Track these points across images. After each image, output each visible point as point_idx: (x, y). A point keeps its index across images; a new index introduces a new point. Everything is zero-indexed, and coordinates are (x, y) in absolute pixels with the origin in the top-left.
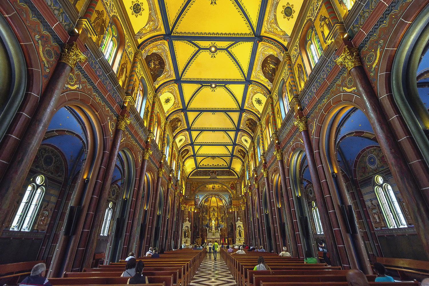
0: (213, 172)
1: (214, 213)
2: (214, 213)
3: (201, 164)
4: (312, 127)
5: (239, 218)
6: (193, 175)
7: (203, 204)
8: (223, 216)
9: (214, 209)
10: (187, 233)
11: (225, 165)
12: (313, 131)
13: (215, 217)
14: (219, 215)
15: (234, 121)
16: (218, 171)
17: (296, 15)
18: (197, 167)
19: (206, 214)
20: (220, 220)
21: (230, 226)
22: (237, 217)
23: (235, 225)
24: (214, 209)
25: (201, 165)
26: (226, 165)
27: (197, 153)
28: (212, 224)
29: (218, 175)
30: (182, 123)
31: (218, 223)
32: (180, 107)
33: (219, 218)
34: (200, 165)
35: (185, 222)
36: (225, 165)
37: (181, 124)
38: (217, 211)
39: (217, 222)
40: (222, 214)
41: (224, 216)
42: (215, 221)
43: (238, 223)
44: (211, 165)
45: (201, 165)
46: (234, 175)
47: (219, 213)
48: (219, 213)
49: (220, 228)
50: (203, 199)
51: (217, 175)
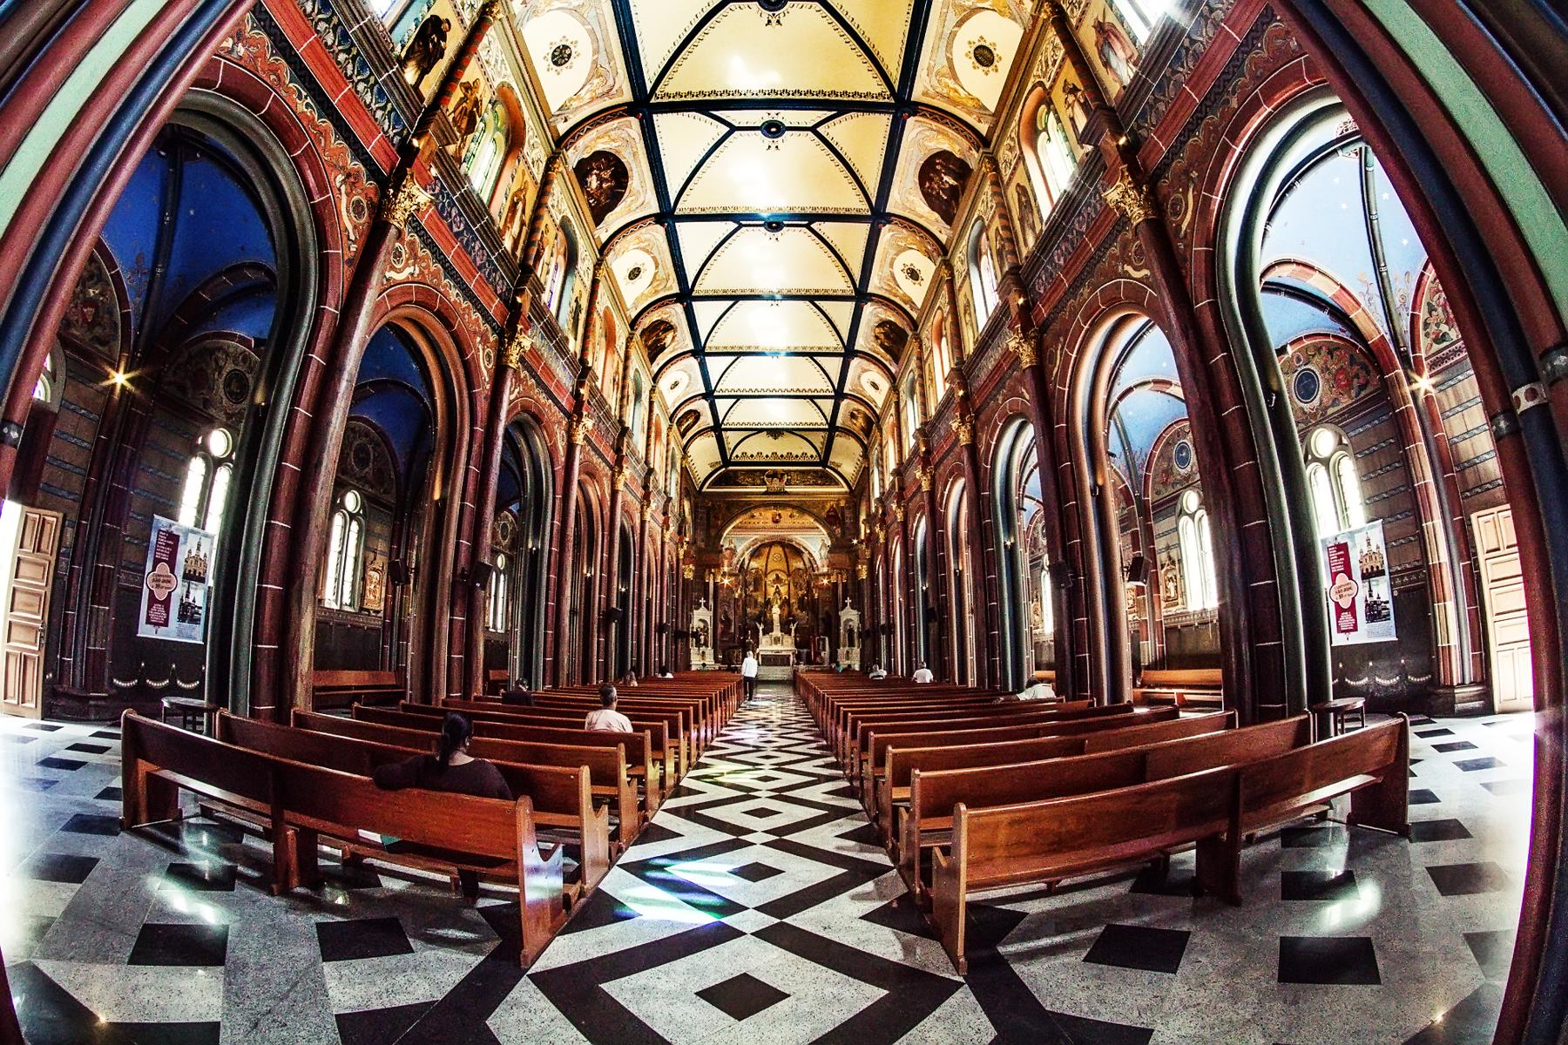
0: (774, 475)
3: (738, 452)
5: (848, 601)
6: (713, 485)
7: (747, 562)
8: (803, 596)
9: (777, 575)
10: (702, 637)
11: (812, 456)
14: (792, 592)
15: (830, 376)
16: (788, 472)
18: (726, 461)
19: (756, 590)
20: (796, 606)
22: (845, 598)
23: (838, 618)
24: (777, 575)
25: (737, 456)
26: (815, 454)
28: (771, 616)
29: (788, 483)
30: (678, 334)
32: (671, 287)
33: (792, 601)
34: (734, 455)
36: (812, 456)
37: (674, 338)
39: (786, 609)
42: (780, 607)
44: (767, 456)
45: (737, 456)
46: (837, 483)
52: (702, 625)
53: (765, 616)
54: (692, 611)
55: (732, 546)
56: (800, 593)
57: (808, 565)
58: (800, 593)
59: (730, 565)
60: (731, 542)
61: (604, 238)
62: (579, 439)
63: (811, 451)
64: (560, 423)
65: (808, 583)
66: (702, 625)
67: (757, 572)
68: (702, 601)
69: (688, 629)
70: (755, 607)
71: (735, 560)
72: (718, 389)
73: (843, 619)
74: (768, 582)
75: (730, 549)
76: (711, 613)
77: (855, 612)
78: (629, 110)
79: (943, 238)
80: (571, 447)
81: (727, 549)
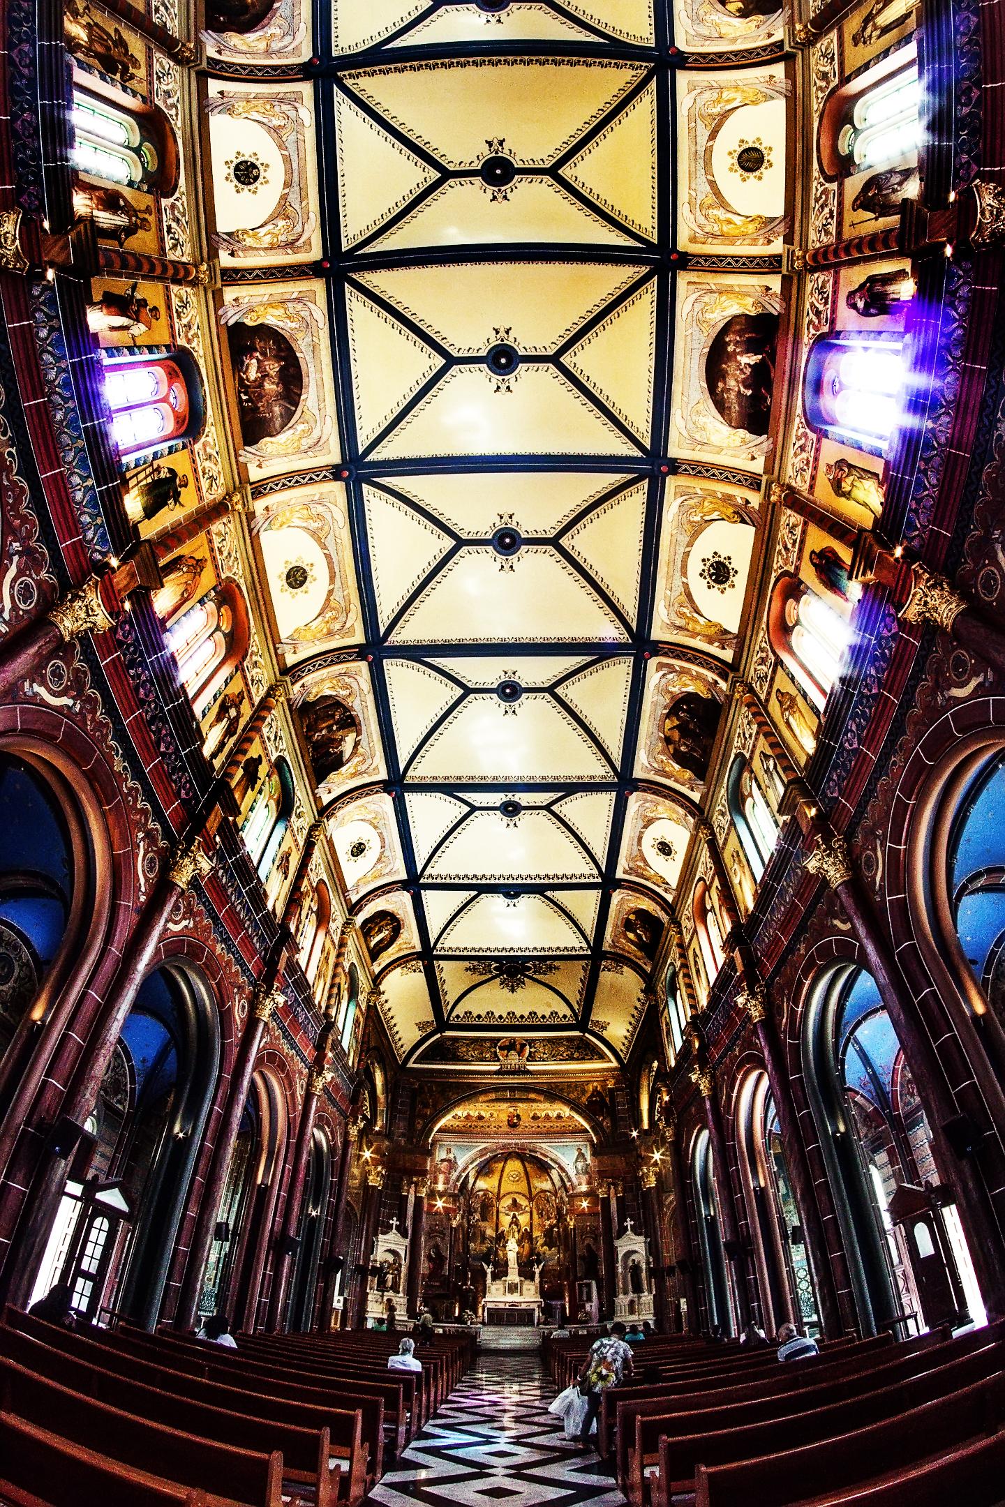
0: (511, 1046)
1: (514, 1216)
2: (514, 1216)
3: (460, 1010)
4: (871, 864)
5: (629, 1223)
6: (421, 1059)
7: (471, 1180)
8: (552, 1227)
9: (515, 1201)
10: (390, 1277)
11: (565, 1016)
12: (878, 879)
13: (519, 1231)
16: (531, 1042)
17: (741, 580)
18: (441, 1021)
19: (484, 1218)
20: (541, 1241)
21: (583, 1258)
22: (622, 1219)
23: (612, 1252)
24: (515, 1201)
25: (458, 1016)
26: (569, 1013)
27: (439, 946)
29: (532, 1058)
30: (363, 737)
31: (532, 1251)
32: (352, 631)
33: (536, 1234)
34: (454, 1014)
35: (384, 1233)
36: (565, 1016)
37: (357, 744)
38: (528, 1209)
39: (527, 1246)
40: (549, 1218)
41: (556, 1225)
42: (519, 1242)
43: (624, 1238)
44: (501, 1017)
45: (458, 1016)
46: (602, 1057)
47: (535, 1216)
48: (535, 1216)
49: (541, 1267)
50: (471, 1163)
51: (528, 1060)
52: (390, 1258)
53: (496, 1254)
54: (376, 1235)
55: (451, 1156)
56: (548, 1223)
57: (558, 1184)
58: (548, 1223)
59: (447, 1182)
60: (449, 1151)
61: (326, 799)
62: (265, 1014)
63: (563, 1010)
64: (241, 988)
65: (559, 1210)
66: (390, 1258)
67: (484, 1195)
68: (394, 1222)
69: (367, 1259)
70: (483, 1242)
71: (454, 1175)
72: (427, 873)
73: (621, 1252)
74: (501, 1209)
75: (449, 1161)
76: (407, 1242)
77: (642, 1238)
78: (360, 652)
79: (696, 796)
80: (252, 1023)
81: (443, 1161)
